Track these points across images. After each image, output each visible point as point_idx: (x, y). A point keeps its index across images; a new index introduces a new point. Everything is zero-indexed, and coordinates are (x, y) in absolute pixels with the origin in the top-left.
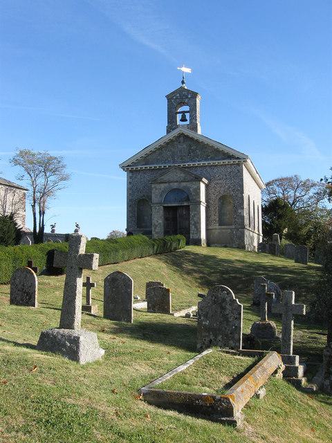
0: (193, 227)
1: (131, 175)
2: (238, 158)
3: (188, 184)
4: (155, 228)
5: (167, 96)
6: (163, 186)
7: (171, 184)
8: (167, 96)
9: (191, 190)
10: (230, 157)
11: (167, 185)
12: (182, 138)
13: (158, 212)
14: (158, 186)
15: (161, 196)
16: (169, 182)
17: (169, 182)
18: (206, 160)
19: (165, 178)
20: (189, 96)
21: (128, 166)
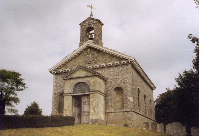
0: (92, 110)
1: (56, 76)
2: (126, 59)
3: (89, 79)
4: (66, 112)
5: (80, 24)
6: (72, 81)
7: (78, 79)
8: (80, 24)
9: (91, 82)
10: (123, 59)
11: (74, 80)
12: (89, 49)
13: (68, 100)
14: (69, 81)
15: (70, 88)
16: (76, 78)
17: (76, 78)
18: (105, 62)
19: (74, 75)
20: (94, 23)
21: (54, 70)
